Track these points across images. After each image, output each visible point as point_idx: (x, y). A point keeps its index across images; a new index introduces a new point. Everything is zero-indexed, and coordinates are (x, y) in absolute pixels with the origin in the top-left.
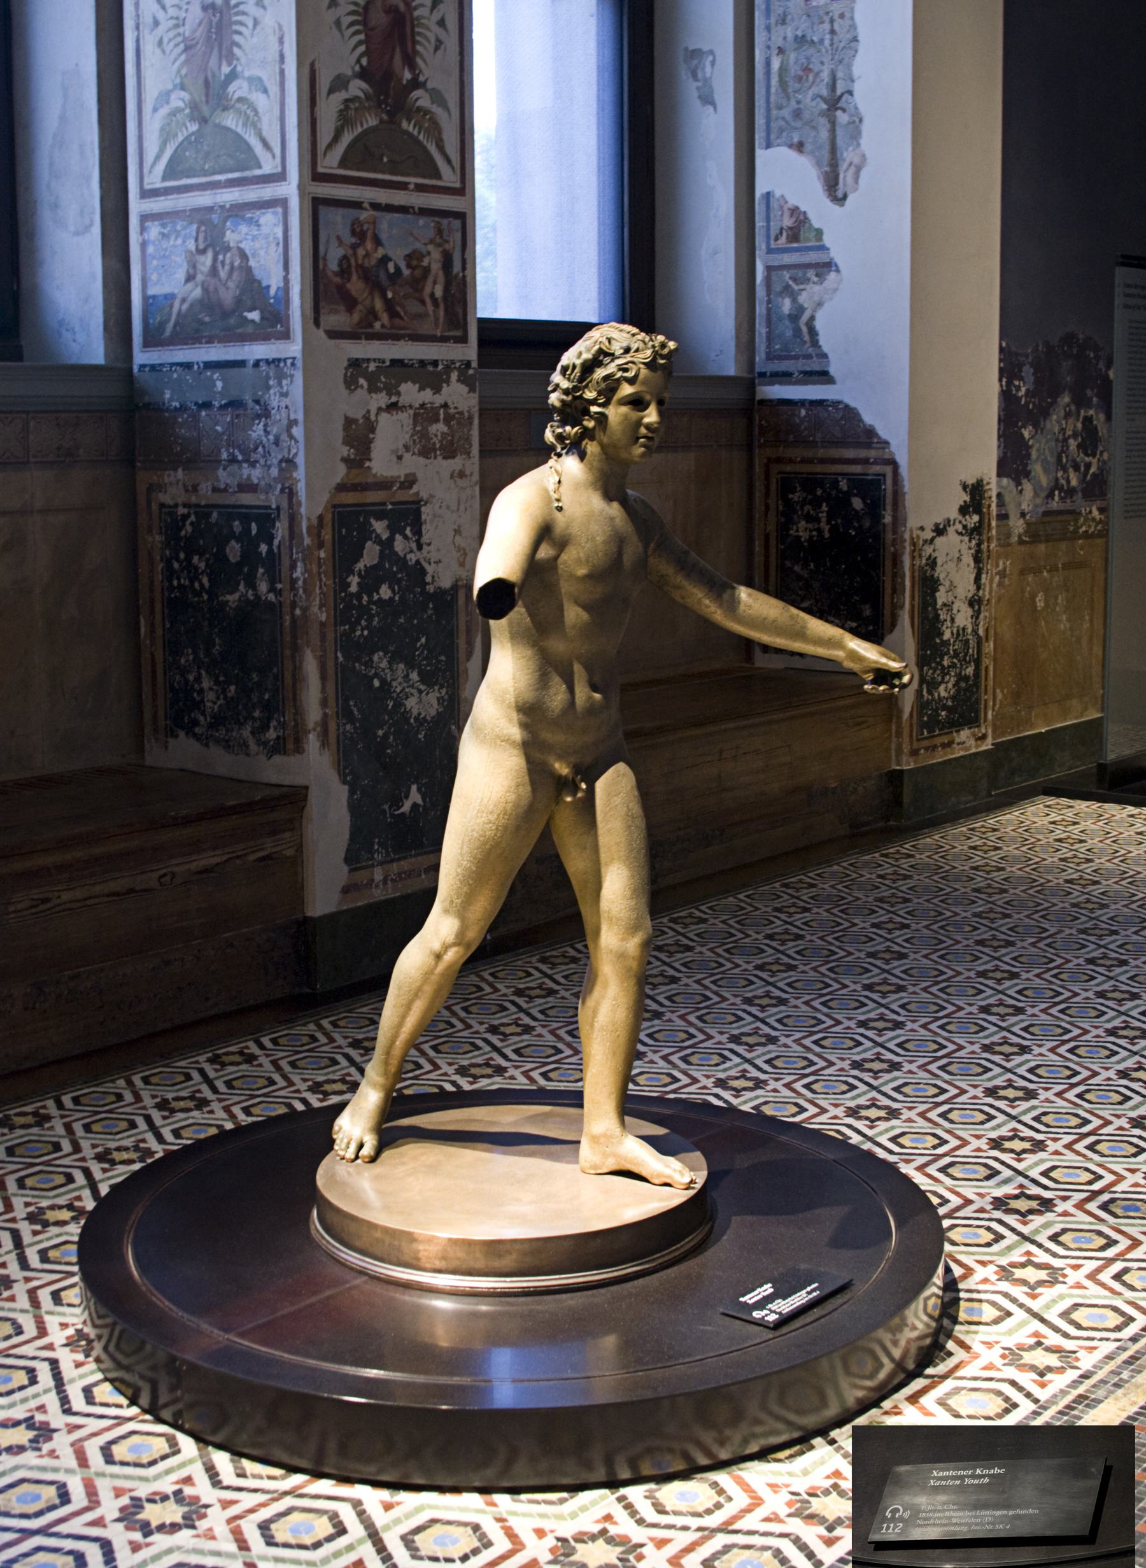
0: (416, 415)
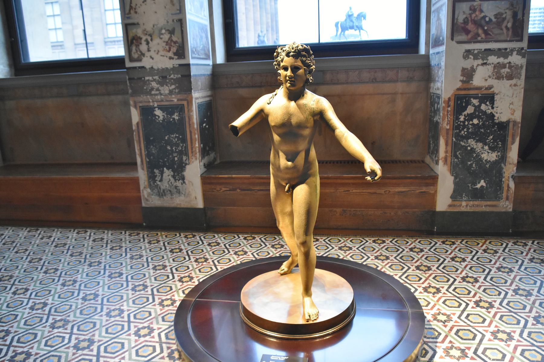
0: (494, 66)
